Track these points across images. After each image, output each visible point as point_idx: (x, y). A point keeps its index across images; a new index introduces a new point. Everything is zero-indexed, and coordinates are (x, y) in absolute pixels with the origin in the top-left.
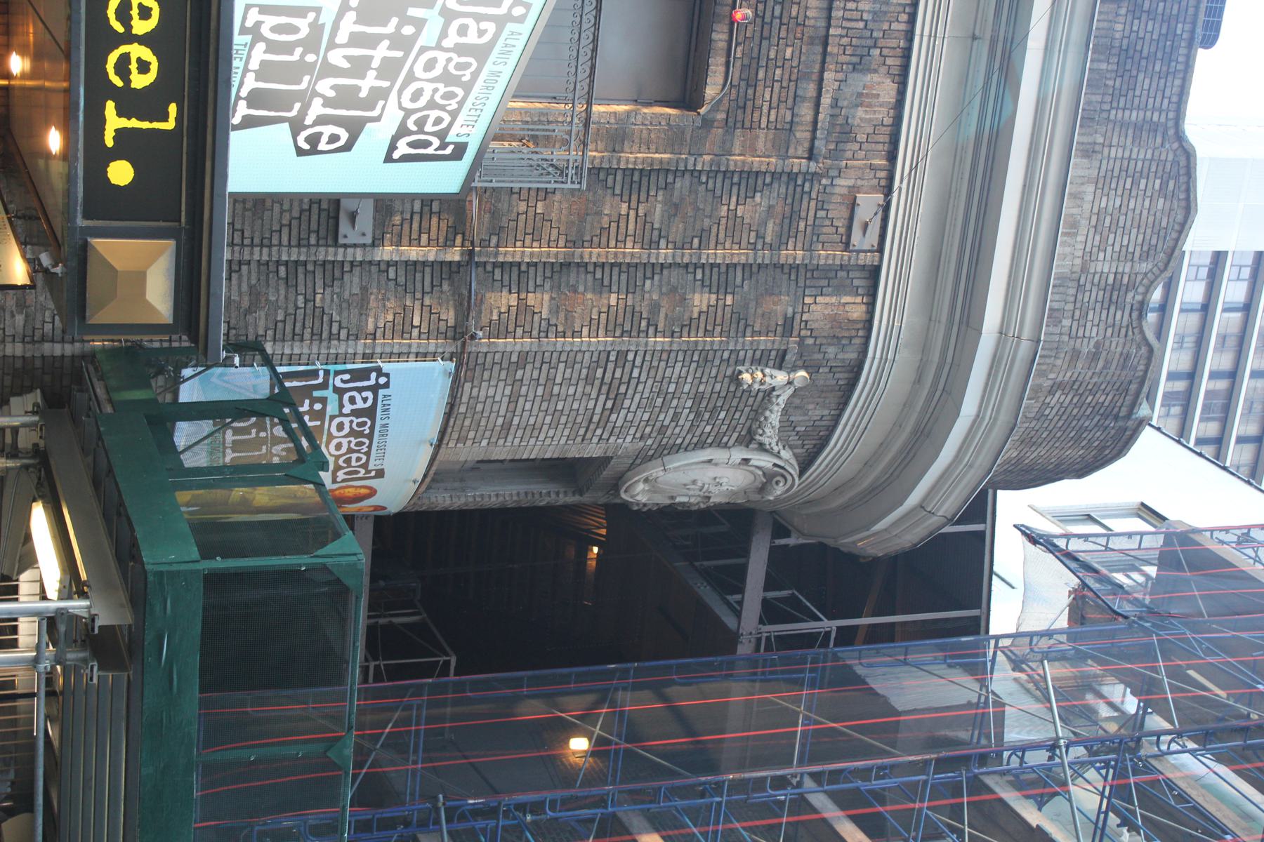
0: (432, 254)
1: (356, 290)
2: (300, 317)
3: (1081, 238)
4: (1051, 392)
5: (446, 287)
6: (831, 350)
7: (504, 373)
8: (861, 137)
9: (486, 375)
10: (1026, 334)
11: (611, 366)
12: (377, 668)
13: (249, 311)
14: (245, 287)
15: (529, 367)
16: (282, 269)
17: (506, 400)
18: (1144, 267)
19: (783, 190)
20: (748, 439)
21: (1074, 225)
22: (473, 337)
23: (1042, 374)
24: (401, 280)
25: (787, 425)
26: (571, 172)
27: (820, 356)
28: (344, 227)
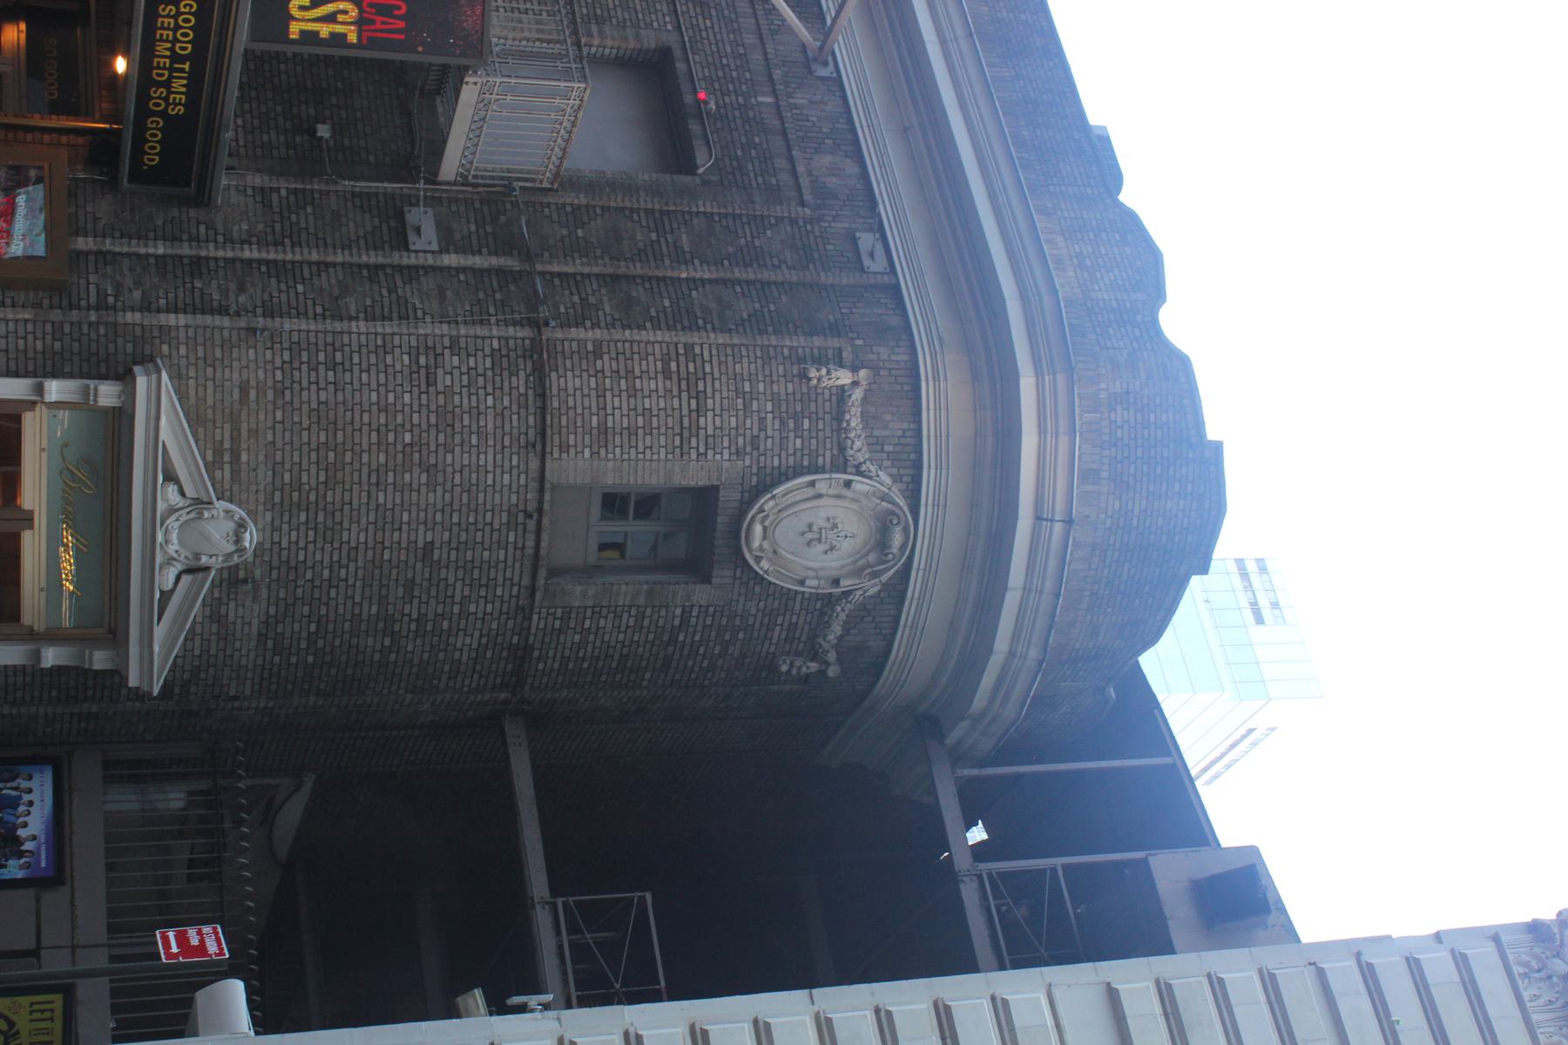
0: (494, 261)
2: (387, 304)
6: (882, 350)
7: (584, 362)
9: (568, 362)
11: (682, 359)
12: (565, 904)
13: (337, 298)
14: (333, 281)
15: (606, 357)
16: (365, 273)
17: (593, 393)
19: (789, 228)
22: (547, 324)
24: (472, 282)
25: (875, 444)
27: (874, 357)
28: (412, 237)
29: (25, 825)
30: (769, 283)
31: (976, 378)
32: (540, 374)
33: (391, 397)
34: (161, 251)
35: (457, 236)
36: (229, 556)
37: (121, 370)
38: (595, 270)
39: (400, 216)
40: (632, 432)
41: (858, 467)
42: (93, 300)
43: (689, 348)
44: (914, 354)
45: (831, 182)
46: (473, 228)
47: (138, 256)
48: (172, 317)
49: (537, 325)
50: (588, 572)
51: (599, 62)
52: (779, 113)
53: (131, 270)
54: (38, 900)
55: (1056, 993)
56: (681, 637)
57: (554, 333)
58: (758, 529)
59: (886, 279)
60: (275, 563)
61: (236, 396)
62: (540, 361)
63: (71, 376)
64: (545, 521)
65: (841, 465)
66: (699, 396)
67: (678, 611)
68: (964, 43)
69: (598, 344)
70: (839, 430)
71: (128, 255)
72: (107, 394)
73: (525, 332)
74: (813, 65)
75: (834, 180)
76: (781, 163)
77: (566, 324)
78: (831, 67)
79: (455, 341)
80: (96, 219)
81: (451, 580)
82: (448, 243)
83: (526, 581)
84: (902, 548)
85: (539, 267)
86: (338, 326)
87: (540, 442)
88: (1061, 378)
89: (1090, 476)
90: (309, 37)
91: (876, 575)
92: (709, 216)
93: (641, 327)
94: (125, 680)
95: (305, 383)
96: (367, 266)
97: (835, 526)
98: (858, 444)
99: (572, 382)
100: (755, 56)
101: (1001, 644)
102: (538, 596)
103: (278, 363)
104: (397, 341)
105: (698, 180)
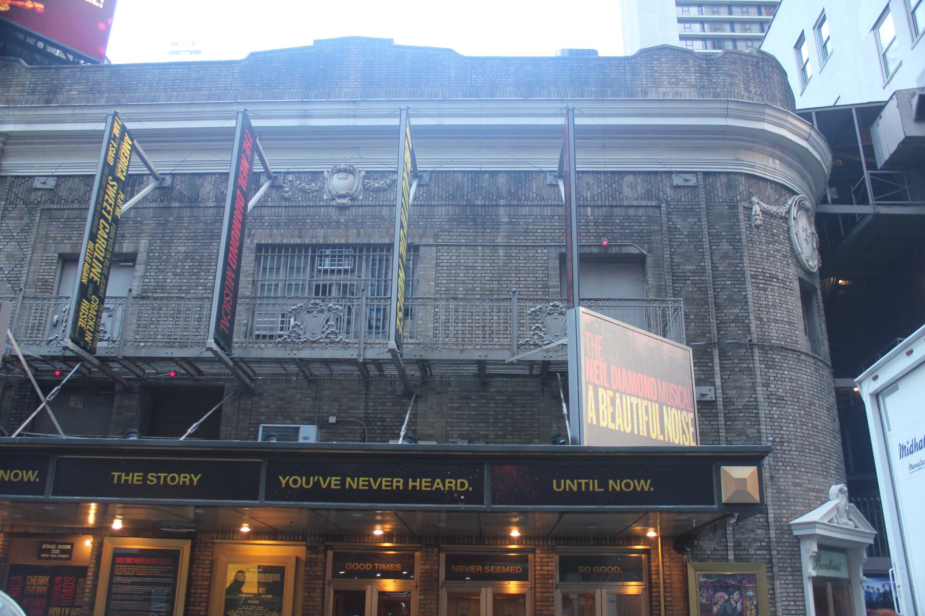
0: (716, 360)
1: (734, 392)
3: (682, 90)
4: (750, 92)
5: (730, 354)
8: (649, 187)
10: (725, 106)
13: (748, 436)
18: (691, 62)
20: (786, 219)
21: (676, 94)
22: (750, 341)
23: (742, 97)
24: (729, 373)
25: (776, 203)
26: (676, 305)
28: (708, 398)
29: (878, 589)
35: (703, 376)
42: (765, 552)
43: (753, 277)
44: (741, 174)
49: (751, 345)
52: (598, 206)
53: (743, 534)
61: (798, 488)
66: (772, 277)
75: (639, 189)
76: (631, 212)
79: (764, 385)
88: (768, 111)
92: (672, 254)
93: (745, 297)
94: (871, 545)
105: (649, 255)
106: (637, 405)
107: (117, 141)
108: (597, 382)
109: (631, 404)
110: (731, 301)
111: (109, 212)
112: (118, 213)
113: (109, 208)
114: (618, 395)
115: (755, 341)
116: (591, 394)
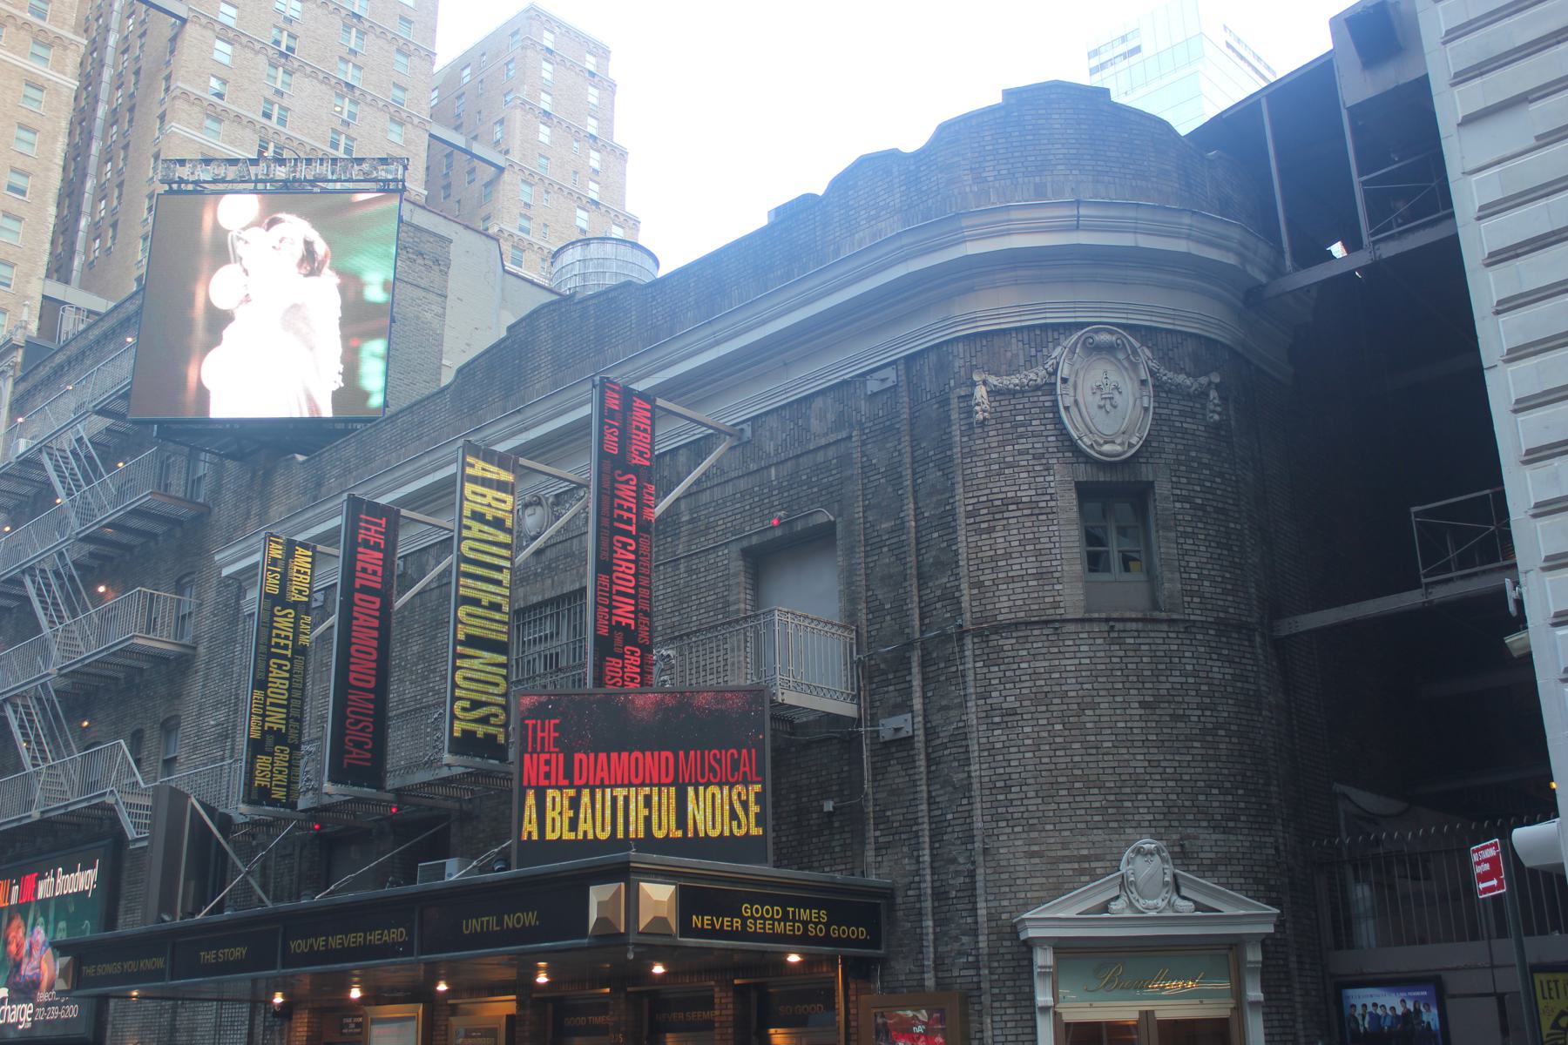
0: (916, 670)
4: (985, 180)
10: (898, 244)
25: (1031, 362)
28: (903, 734)
29: (1393, 1009)
30: (913, 457)
31: (971, 290)
32: (998, 629)
33: (1028, 742)
34: (930, 923)
36: (1163, 860)
37: (1024, 949)
38: (915, 591)
39: (887, 744)
40: (1038, 553)
41: (1050, 374)
42: (972, 972)
43: (969, 515)
44: (957, 339)
45: (831, 417)
46: (891, 688)
47: (935, 940)
48: (980, 912)
49: (962, 634)
50: (1152, 579)
51: (757, 601)
54: (1454, 996)
55: (1470, 167)
56: (1199, 501)
57: (967, 620)
58: (1107, 448)
59: (901, 367)
60: (1166, 823)
61: (1037, 860)
62: (989, 630)
63: (1032, 986)
64: (1115, 615)
65: (1050, 388)
66: (1006, 503)
67: (1178, 505)
68: (717, 327)
69: (972, 586)
70: (1022, 392)
71: (935, 947)
72: (1044, 958)
73: (968, 642)
74: (743, 440)
77: (959, 611)
78: (744, 426)
79: (980, 696)
80: (911, 972)
81: (1168, 686)
82: (904, 707)
83: (1165, 627)
84: (1111, 332)
85: (917, 635)
86: (976, 786)
87: (1054, 624)
88: (965, 222)
89: (1040, 191)
90: (760, 819)
91: (1135, 352)
92: (866, 509)
95: (1022, 809)
96: (928, 766)
97: (1099, 387)
98: (1032, 376)
99: (1004, 603)
100: (743, 484)
101: (1181, 246)
102: (1175, 616)
103: (1009, 830)
104: (984, 740)
106: (626, 799)
107: (281, 563)
108: (543, 783)
109: (614, 799)
110: (940, 565)
111: (286, 647)
112: (303, 640)
113: (283, 642)
114: (586, 792)
115: (968, 626)
116: (531, 800)
